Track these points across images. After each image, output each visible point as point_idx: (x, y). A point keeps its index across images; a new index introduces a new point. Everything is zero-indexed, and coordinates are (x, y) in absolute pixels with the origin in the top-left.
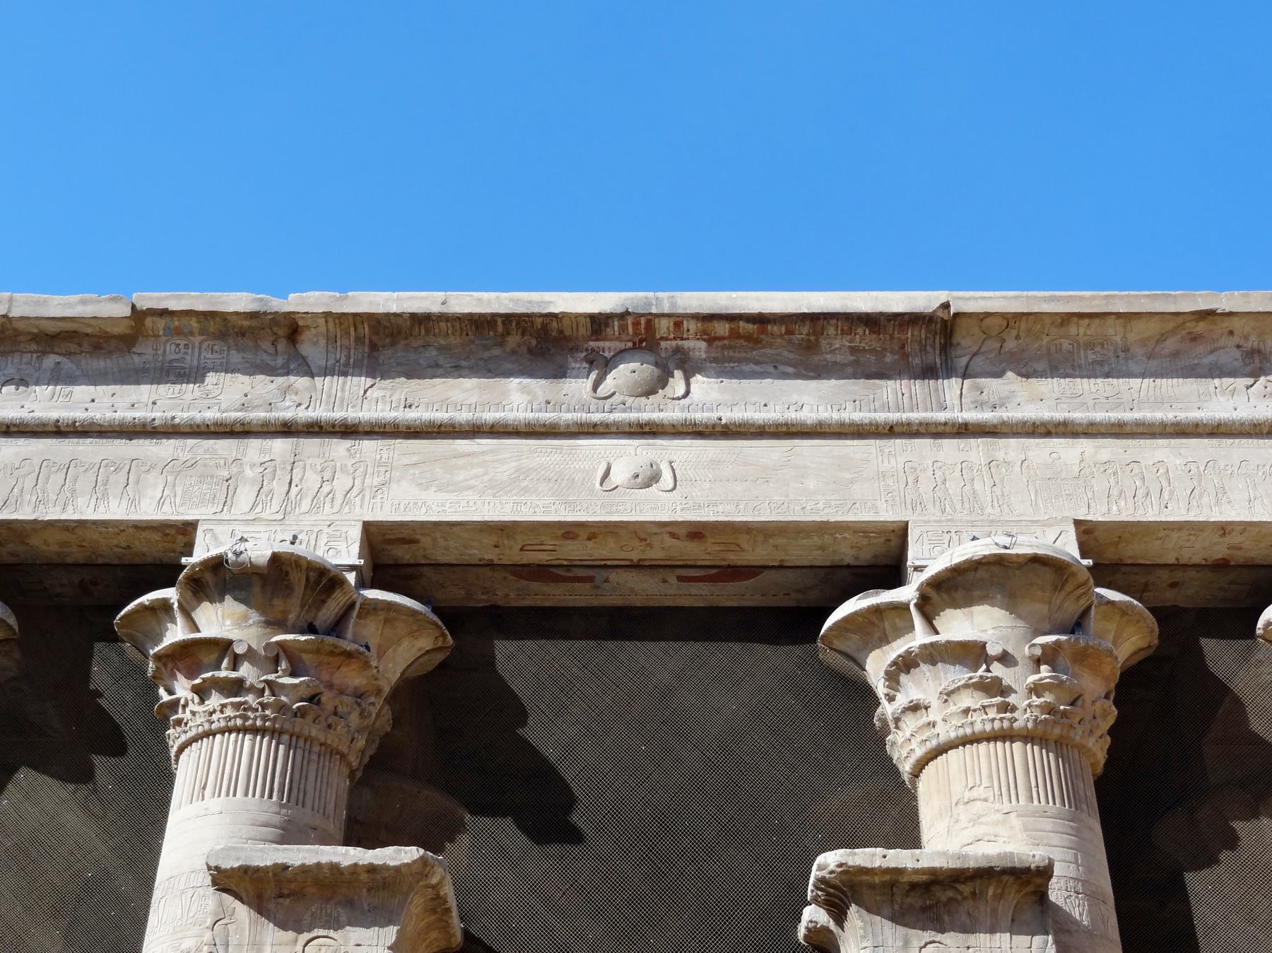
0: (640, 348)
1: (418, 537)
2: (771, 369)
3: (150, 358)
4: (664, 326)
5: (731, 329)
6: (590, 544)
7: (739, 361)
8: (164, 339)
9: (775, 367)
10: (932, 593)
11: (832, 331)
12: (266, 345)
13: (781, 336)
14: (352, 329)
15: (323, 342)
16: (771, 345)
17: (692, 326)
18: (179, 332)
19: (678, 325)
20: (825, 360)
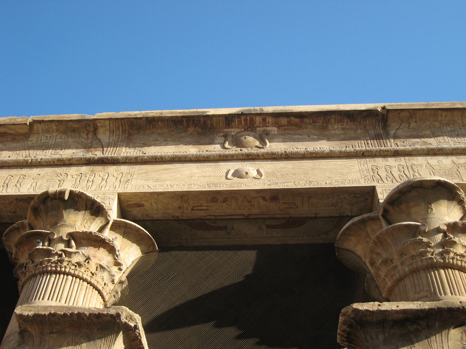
0: (247, 131)
1: (143, 202)
2: (307, 137)
3: (35, 142)
4: (258, 119)
5: (288, 121)
6: (224, 205)
7: (292, 134)
8: (41, 134)
9: (309, 136)
10: (390, 208)
11: (333, 121)
12: (84, 135)
13: (310, 124)
14: (121, 127)
15: (108, 133)
16: (306, 128)
17: (270, 120)
18: (48, 131)
19: (264, 120)
20: (331, 133)
